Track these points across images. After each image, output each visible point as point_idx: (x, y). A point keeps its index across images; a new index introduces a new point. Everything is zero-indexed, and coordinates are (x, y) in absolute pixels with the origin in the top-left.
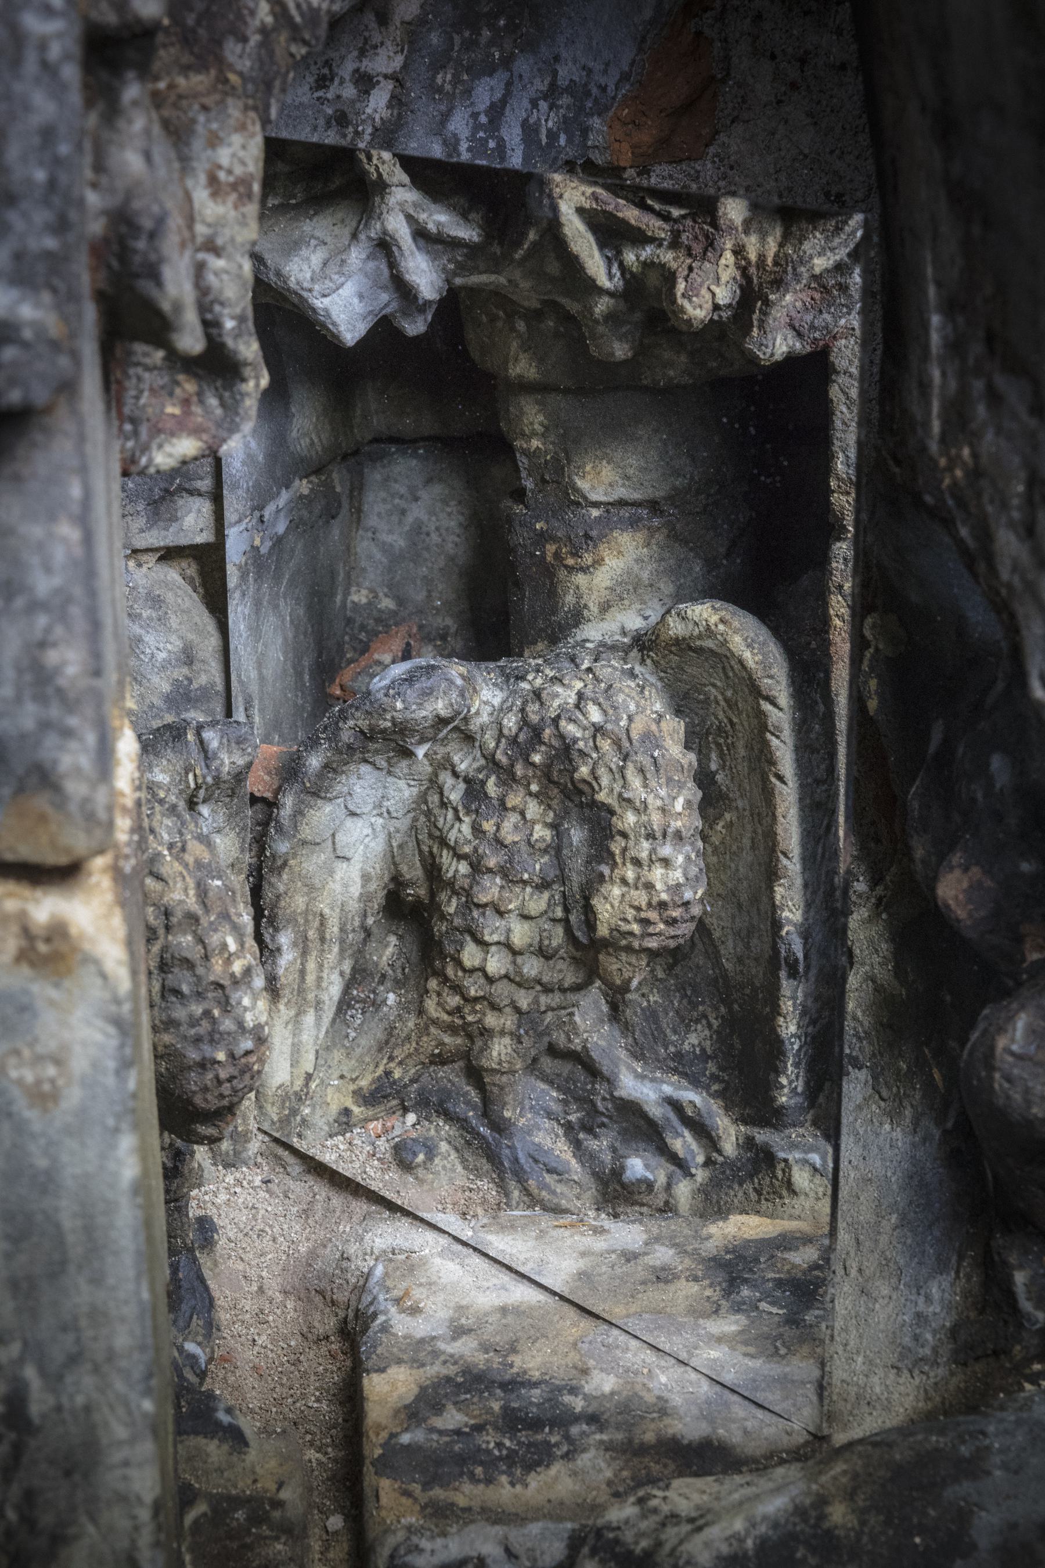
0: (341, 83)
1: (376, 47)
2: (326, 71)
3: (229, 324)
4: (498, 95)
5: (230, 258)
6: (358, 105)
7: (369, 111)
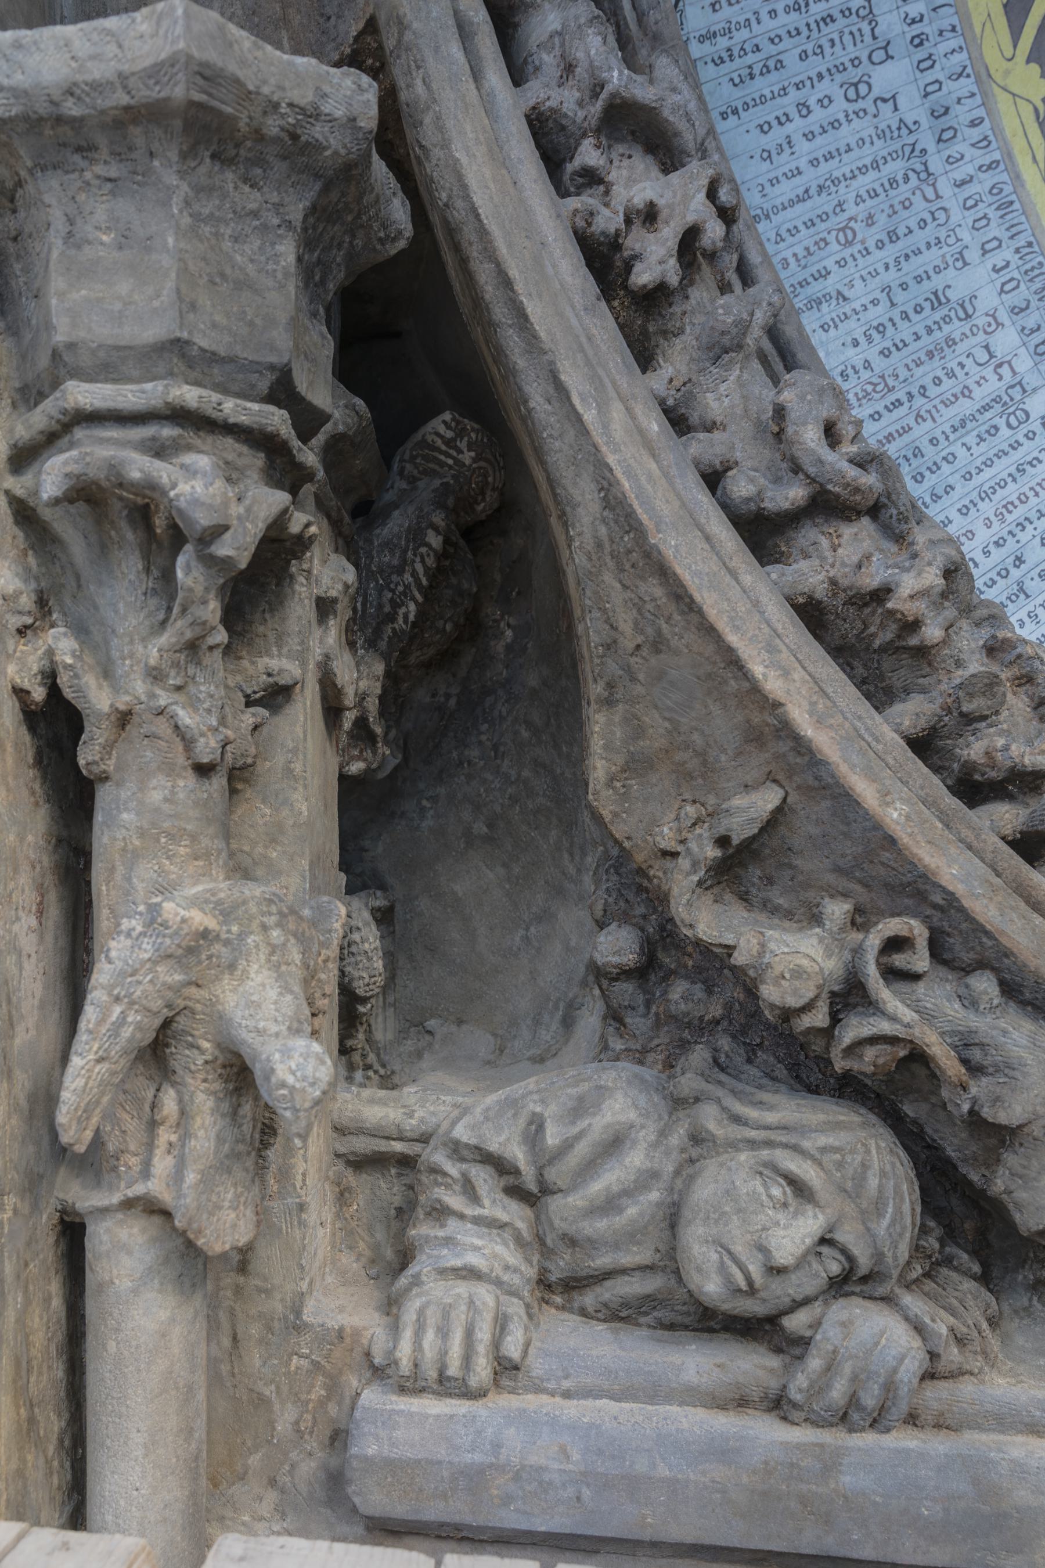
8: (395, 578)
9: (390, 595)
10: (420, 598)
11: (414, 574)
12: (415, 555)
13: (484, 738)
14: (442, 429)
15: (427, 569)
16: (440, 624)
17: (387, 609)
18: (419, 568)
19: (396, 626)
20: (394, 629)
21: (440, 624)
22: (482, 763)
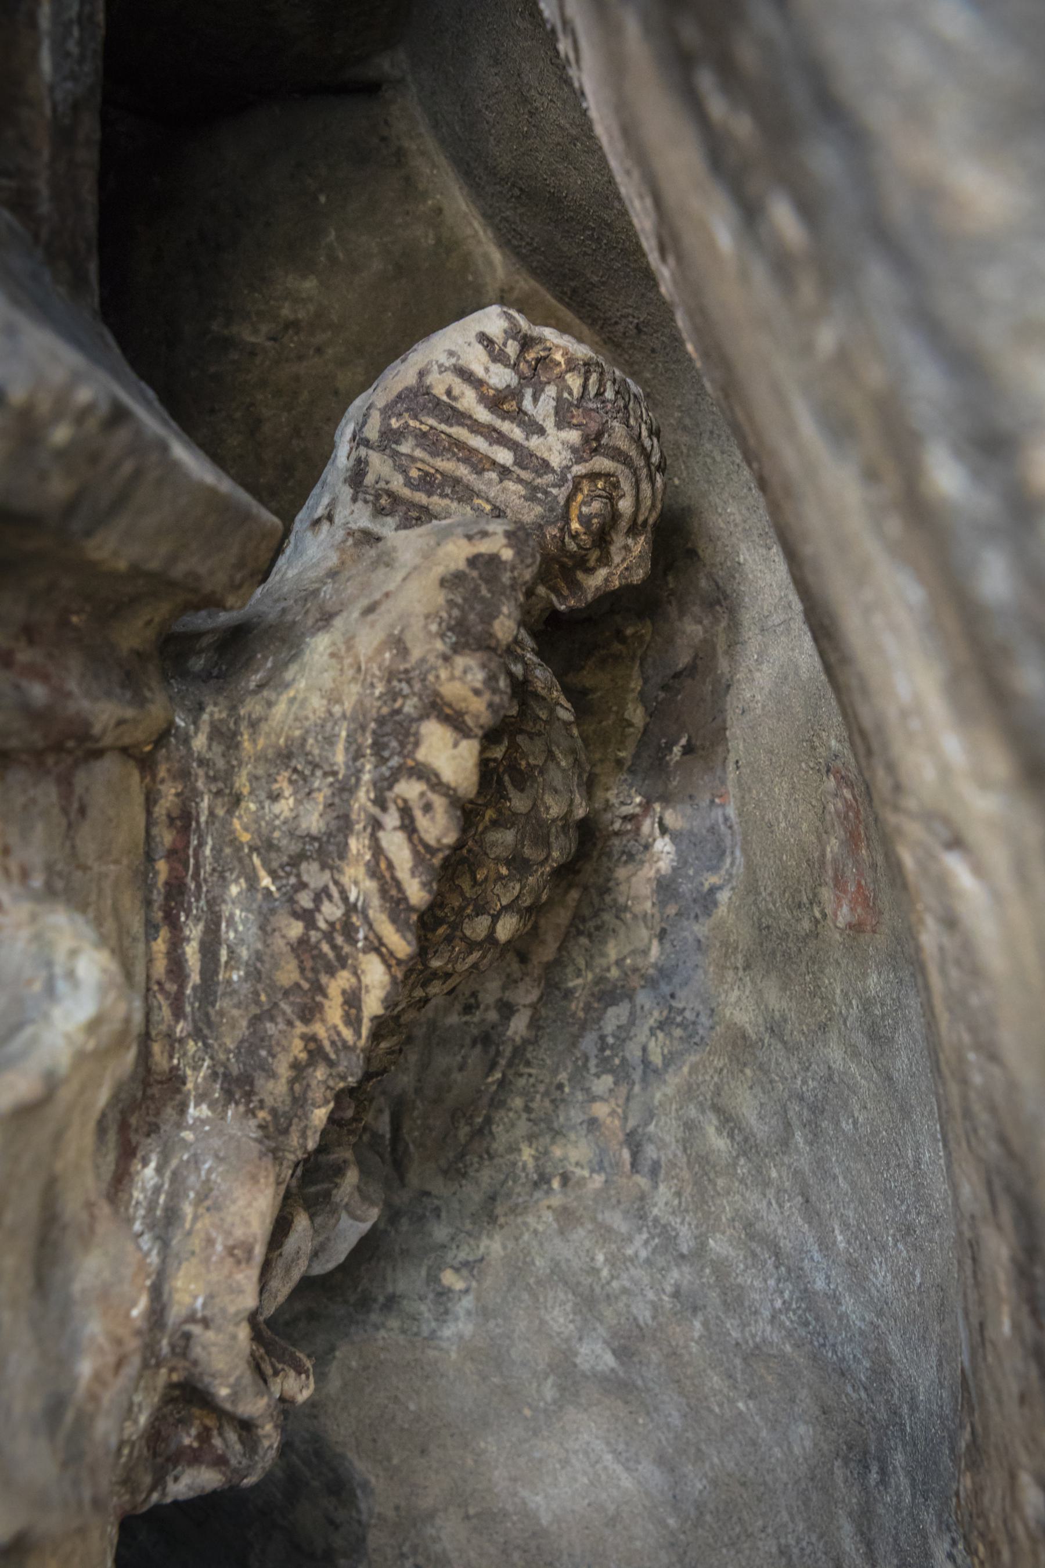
1: (516, 982)
2: (472, 1001)
4: (624, 1020)
5: (219, 1330)
6: (500, 1028)
7: (509, 1033)
8: (314, 875)
9: (296, 929)
10: (400, 945)
11: (379, 867)
12: (381, 803)
13: (600, 1110)
14: (477, 360)
15: (422, 851)
16: (478, 928)
17: (288, 974)
18: (398, 849)
19: (319, 1029)
20: (310, 1039)
21: (478, 928)
22: (598, 1181)
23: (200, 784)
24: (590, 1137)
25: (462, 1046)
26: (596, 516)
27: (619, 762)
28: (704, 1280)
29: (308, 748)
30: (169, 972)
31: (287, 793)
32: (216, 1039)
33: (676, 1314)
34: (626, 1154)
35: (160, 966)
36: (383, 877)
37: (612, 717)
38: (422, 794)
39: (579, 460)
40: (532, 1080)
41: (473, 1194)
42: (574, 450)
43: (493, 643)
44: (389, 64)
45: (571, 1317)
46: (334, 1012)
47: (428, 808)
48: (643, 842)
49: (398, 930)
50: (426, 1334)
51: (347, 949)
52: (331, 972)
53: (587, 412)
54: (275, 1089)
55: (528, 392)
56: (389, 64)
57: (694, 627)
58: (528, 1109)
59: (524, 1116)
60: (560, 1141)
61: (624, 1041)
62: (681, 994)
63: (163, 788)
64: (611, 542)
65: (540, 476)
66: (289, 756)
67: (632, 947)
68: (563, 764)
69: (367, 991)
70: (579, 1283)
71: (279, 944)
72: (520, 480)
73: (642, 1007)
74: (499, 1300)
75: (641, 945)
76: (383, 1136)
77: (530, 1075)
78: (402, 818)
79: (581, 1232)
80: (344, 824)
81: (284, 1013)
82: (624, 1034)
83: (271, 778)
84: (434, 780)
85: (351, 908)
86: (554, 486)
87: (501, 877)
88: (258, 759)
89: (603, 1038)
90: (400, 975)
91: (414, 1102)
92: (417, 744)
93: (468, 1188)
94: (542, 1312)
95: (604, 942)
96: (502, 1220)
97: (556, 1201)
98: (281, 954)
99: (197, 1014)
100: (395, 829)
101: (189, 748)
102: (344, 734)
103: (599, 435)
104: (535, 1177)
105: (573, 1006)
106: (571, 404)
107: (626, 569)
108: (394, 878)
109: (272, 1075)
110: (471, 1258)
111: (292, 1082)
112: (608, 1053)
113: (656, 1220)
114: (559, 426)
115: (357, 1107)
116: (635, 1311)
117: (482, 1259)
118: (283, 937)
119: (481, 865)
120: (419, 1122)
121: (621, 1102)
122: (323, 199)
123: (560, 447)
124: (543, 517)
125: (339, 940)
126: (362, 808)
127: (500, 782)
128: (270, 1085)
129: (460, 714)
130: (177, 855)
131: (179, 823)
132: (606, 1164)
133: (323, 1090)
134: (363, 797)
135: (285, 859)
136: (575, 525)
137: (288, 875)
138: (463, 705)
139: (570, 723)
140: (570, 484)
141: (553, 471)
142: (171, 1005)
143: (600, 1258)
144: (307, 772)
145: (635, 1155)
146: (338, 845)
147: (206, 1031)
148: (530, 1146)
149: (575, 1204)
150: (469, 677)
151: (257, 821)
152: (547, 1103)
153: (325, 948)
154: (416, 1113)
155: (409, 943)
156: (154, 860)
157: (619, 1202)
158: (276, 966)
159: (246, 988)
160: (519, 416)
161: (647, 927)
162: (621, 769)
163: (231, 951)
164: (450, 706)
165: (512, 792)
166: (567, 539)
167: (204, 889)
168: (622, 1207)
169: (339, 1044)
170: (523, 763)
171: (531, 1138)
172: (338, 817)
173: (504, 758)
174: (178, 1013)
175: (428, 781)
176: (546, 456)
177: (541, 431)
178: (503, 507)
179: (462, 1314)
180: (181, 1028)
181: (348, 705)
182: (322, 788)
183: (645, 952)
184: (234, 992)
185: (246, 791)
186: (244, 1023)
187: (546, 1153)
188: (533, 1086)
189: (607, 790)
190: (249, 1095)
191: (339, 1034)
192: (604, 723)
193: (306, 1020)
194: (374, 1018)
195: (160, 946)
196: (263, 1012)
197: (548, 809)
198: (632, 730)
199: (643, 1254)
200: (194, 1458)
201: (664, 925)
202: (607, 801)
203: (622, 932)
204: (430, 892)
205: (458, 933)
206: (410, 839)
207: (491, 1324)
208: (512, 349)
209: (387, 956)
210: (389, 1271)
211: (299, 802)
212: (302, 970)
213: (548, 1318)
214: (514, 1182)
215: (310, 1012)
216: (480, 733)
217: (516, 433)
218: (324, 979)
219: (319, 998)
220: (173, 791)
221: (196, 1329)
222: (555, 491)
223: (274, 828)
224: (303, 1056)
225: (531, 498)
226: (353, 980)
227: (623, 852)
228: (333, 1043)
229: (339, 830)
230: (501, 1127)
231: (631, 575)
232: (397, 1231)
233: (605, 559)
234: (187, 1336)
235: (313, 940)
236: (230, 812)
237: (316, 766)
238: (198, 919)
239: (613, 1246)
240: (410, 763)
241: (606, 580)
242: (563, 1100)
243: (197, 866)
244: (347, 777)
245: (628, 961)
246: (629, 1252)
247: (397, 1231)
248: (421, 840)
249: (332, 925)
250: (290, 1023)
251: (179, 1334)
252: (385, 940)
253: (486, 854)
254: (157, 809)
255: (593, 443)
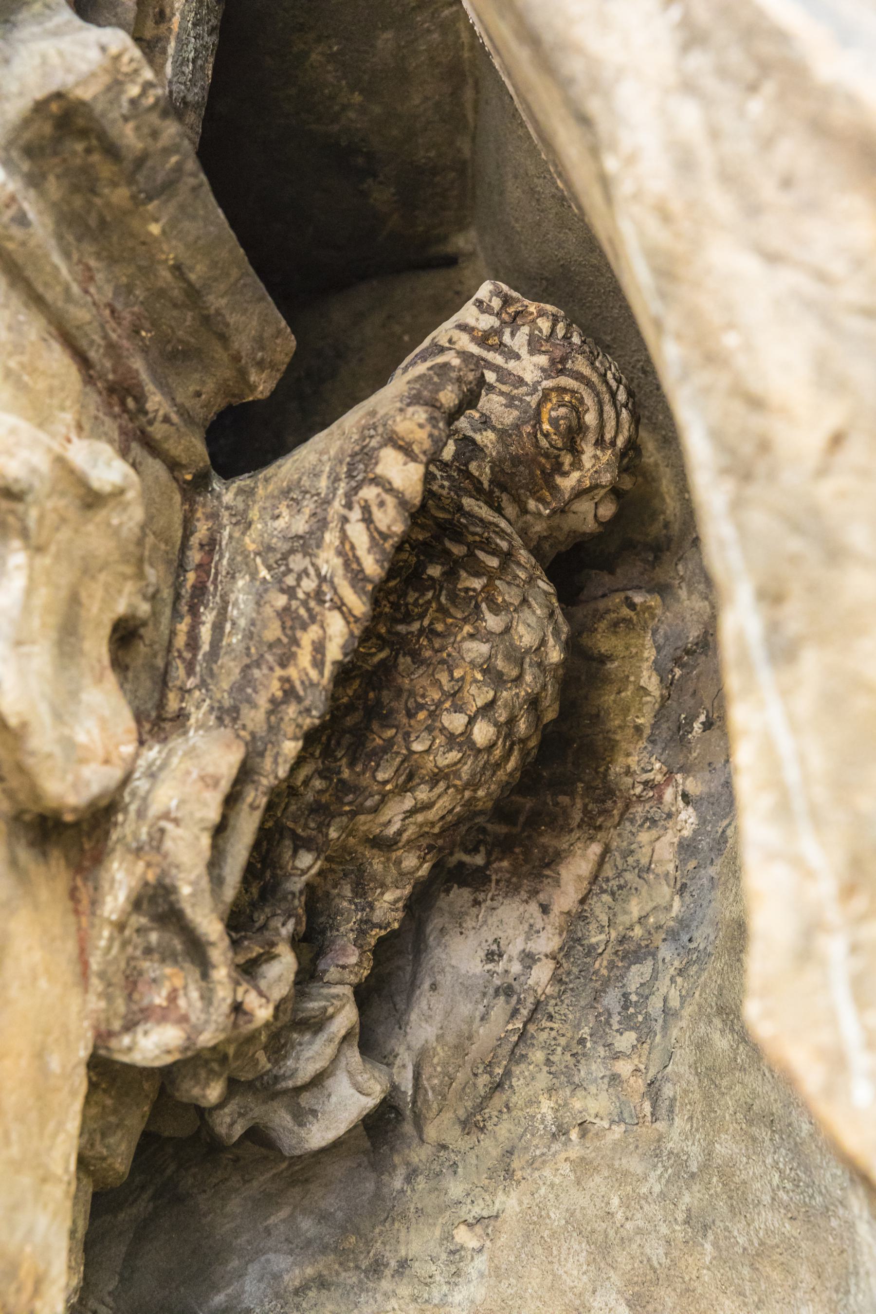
0: (510, 960)
1: (538, 932)
3: (186, 890)
4: (647, 977)
6: (522, 978)
7: (530, 982)
8: (298, 562)
9: (282, 600)
10: (358, 605)
11: (347, 555)
12: (349, 506)
13: (624, 1068)
15: (378, 537)
17: (273, 632)
18: (358, 534)
19: (292, 672)
23: (225, 521)
24: (611, 1090)
25: (484, 994)
26: (562, 418)
27: (638, 729)
28: (712, 1192)
29: (302, 483)
30: (187, 645)
31: (284, 514)
32: (215, 685)
33: (687, 1242)
34: (647, 1107)
35: (181, 641)
36: (347, 555)
37: (631, 687)
38: (378, 495)
39: (548, 377)
40: (554, 1033)
41: (490, 1147)
42: (543, 370)
43: (438, 405)
44: (463, 241)
45: (585, 1267)
46: (304, 657)
47: (382, 504)
48: (666, 810)
49: (356, 592)
50: (436, 1301)
51: (317, 609)
52: (304, 627)
53: (555, 345)
54: (255, 718)
55: (507, 331)
56: (463, 242)
57: (701, 604)
58: (548, 1062)
59: (545, 1069)
60: (580, 1093)
61: (647, 998)
62: (696, 934)
63: (198, 524)
64: (582, 452)
65: (517, 388)
66: (289, 490)
67: (654, 904)
68: (538, 612)
69: (330, 640)
70: (593, 1231)
71: (268, 611)
72: (502, 393)
73: (664, 960)
74: (512, 1259)
75: (663, 902)
76: (405, 1093)
77: (552, 1029)
78: (363, 513)
79: (598, 1179)
80: (323, 524)
81: (267, 662)
82: (647, 989)
83: (275, 507)
84: (388, 486)
85: (322, 579)
86: (527, 395)
87: (476, 681)
88: (267, 497)
89: (626, 995)
90: (357, 632)
91: (434, 1049)
92: (376, 464)
93: (487, 1142)
94: (556, 1266)
95: (626, 901)
96: (518, 1174)
97: (575, 1152)
98: (269, 618)
99: (204, 671)
100: (358, 521)
101: (221, 502)
102: (327, 469)
103: (563, 360)
104: (554, 1129)
105: (597, 965)
106: (541, 338)
107: (596, 472)
108: (354, 556)
109: (254, 706)
110: (485, 1214)
111: (270, 713)
112: (632, 1010)
113: (671, 1152)
114: (532, 352)
115: (360, 955)
116: (648, 1251)
117: (497, 1217)
118: (272, 606)
119: (457, 667)
120: (439, 1069)
121: (644, 1059)
122: (406, 338)
123: (532, 368)
124: (519, 418)
125: (312, 604)
126: (337, 512)
127: (477, 606)
128: (252, 713)
129: (410, 444)
130: (203, 568)
131: (207, 548)
132: (626, 1115)
133: (293, 726)
134: (337, 505)
135: (279, 556)
136: (546, 427)
137: (279, 566)
138: (411, 436)
139: (550, 594)
140: (540, 393)
141: (527, 384)
142: (186, 667)
143: (615, 1201)
144: (300, 498)
145: (654, 1106)
146: (316, 539)
147: (209, 681)
148: (550, 1099)
149: (593, 1154)
150: (416, 416)
151: (262, 535)
152: (568, 1057)
153: (302, 612)
154: (435, 1061)
155: (364, 603)
156: (186, 571)
157: (637, 1147)
158: (265, 627)
159: (241, 647)
160: (500, 348)
161: (669, 886)
162: (641, 736)
163: (234, 624)
164: (403, 439)
165: (488, 615)
166: (539, 436)
167: (220, 588)
168: (640, 1151)
169: (307, 683)
170: (500, 599)
171: (551, 1090)
172: (319, 521)
173: (482, 590)
174: (190, 671)
175: (383, 487)
176: (521, 374)
177: (518, 357)
178: (488, 413)
179: (474, 1275)
180: (191, 683)
181: (332, 453)
182: (309, 505)
183: (668, 908)
184: (233, 650)
185: (255, 518)
186: (237, 671)
187: (566, 1104)
188: (555, 1039)
189: (628, 755)
190: (235, 720)
191: (307, 674)
192: (623, 694)
193: (283, 665)
194: (335, 663)
195: (183, 627)
196: (252, 662)
197: (521, 637)
198: (648, 699)
199: (657, 1189)
200: (163, 1015)
201: (684, 881)
202: (629, 767)
203: (644, 890)
204: (382, 567)
205: (438, 724)
206: (368, 528)
207: (504, 1285)
208: (496, 303)
209: (347, 615)
210: (403, 1235)
211: (292, 516)
212: (284, 628)
213: (561, 1272)
214: (533, 1135)
215: (285, 661)
216: (424, 458)
217: (497, 359)
218: (299, 634)
219: (294, 649)
220: (205, 527)
221: (169, 826)
222: (528, 399)
223: (273, 536)
224: (279, 694)
225: (509, 406)
226: (321, 632)
227: (647, 819)
228: (302, 683)
229: (318, 529)
230: (522, 1081)
231: (600, 478)
232: (413, 1190)
233: (577, 465)
234: (162, 831)
235: (294, 607)
236: (244, 534)
237: (306, 492)
238: (213, 609)
239: (629, 1188)
240: (371, 476)
241: (579, 481)
242: (584, 1055)
243: (216, 574)
244: (327, 495)
245: (652, 920)
246: (644, 1190)
247: (413, 1190)
248: (376, 529)
249: (308, 594)
250: (271, 669)
251: (155, 828)
252: (346, 600)
253: (463, 658)
254: (192, 539)
255: (558, 367)
